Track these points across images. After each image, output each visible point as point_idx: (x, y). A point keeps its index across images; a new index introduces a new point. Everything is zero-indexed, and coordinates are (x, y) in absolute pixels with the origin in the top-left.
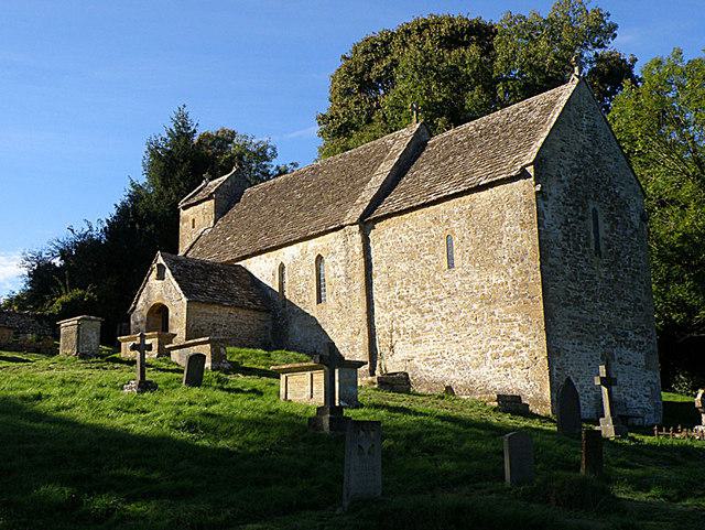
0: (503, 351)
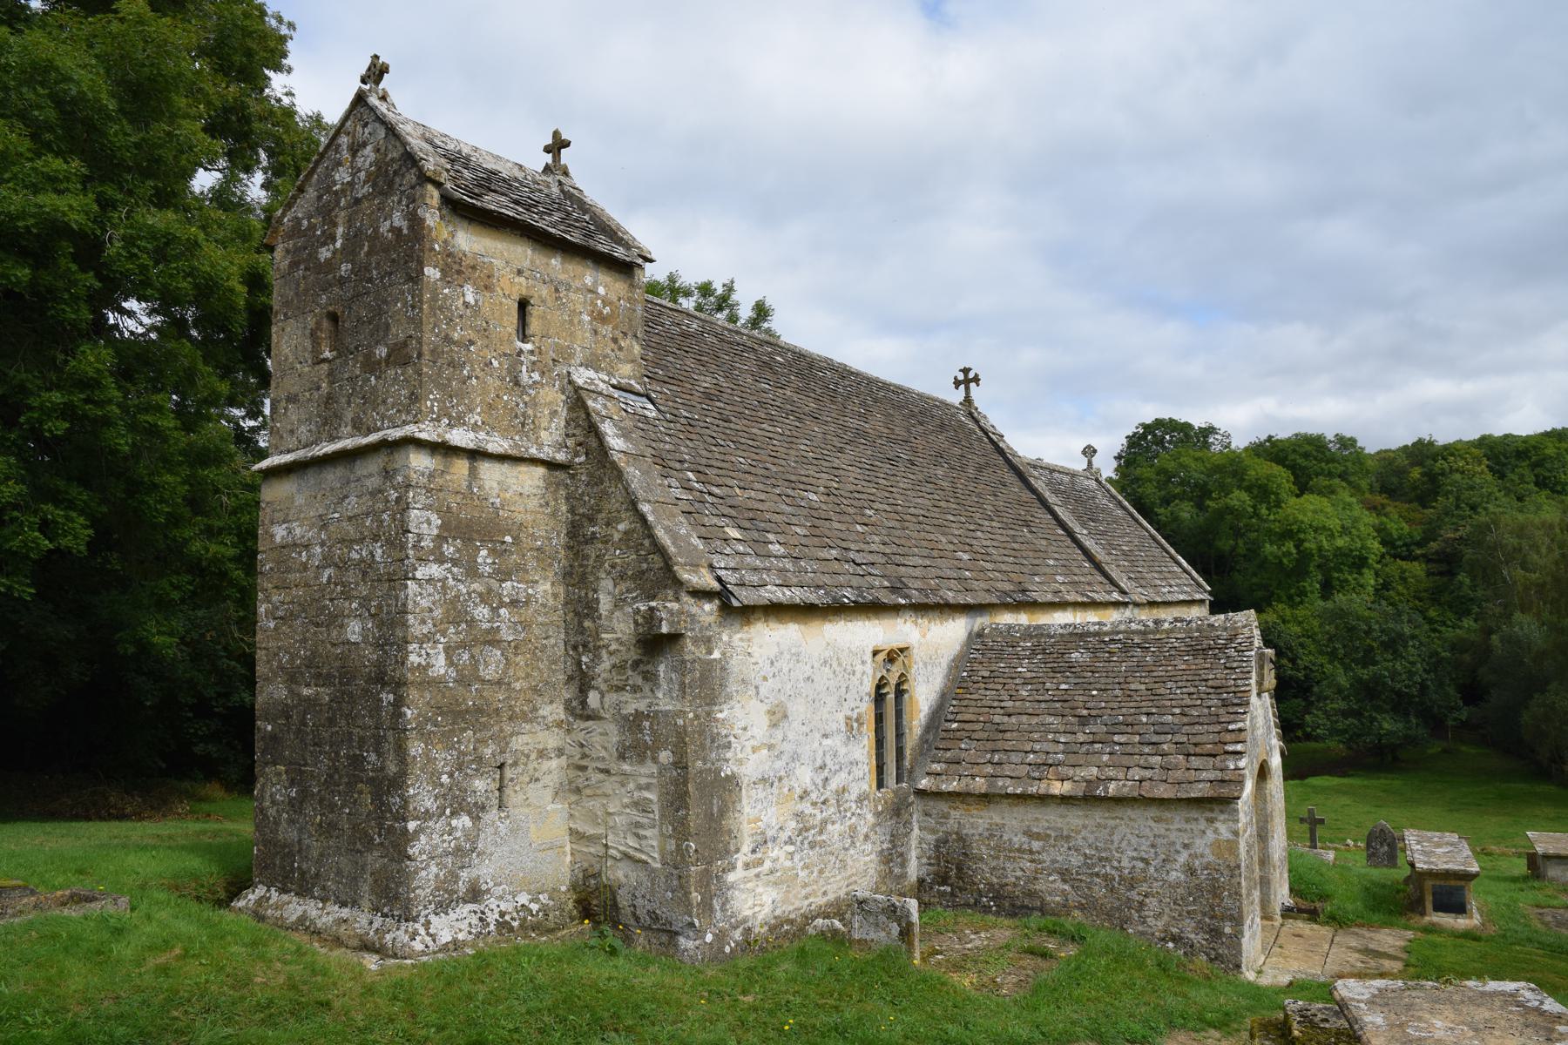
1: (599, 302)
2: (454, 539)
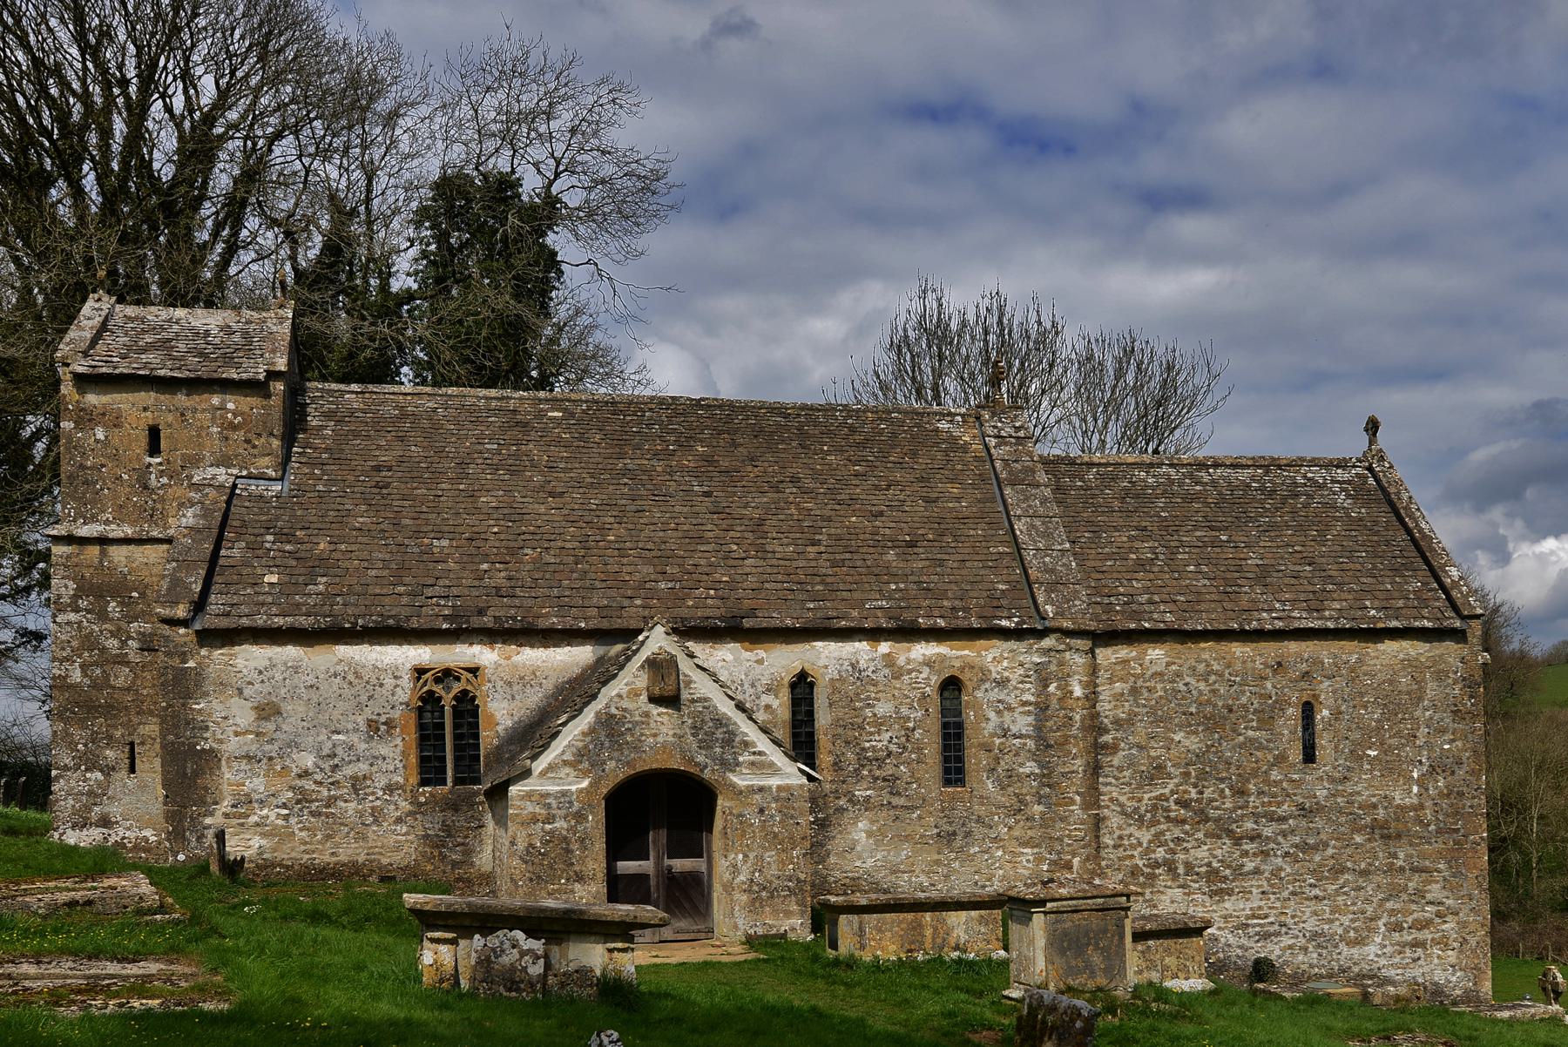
0: (1410, 919)
1: (229, 415)
2: (88, 596)
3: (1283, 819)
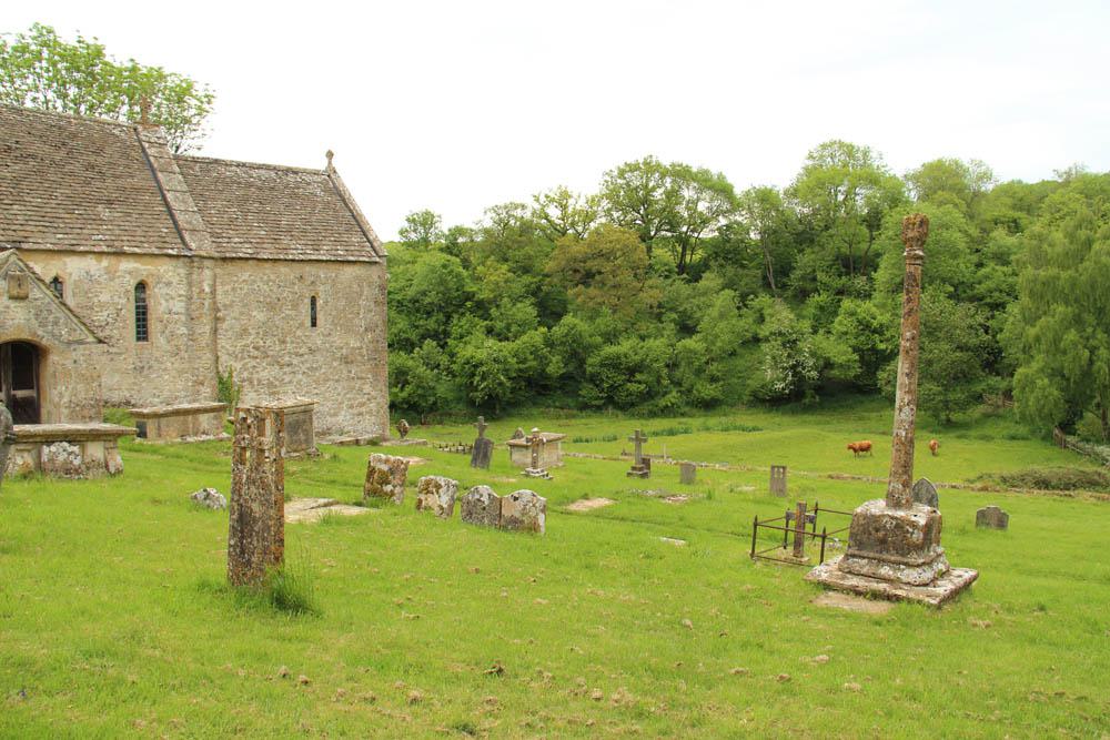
3: (302, 355)
